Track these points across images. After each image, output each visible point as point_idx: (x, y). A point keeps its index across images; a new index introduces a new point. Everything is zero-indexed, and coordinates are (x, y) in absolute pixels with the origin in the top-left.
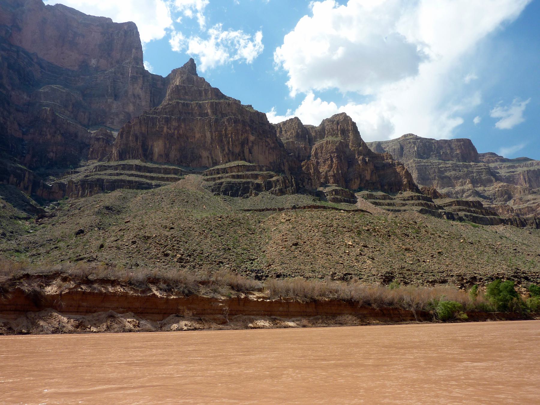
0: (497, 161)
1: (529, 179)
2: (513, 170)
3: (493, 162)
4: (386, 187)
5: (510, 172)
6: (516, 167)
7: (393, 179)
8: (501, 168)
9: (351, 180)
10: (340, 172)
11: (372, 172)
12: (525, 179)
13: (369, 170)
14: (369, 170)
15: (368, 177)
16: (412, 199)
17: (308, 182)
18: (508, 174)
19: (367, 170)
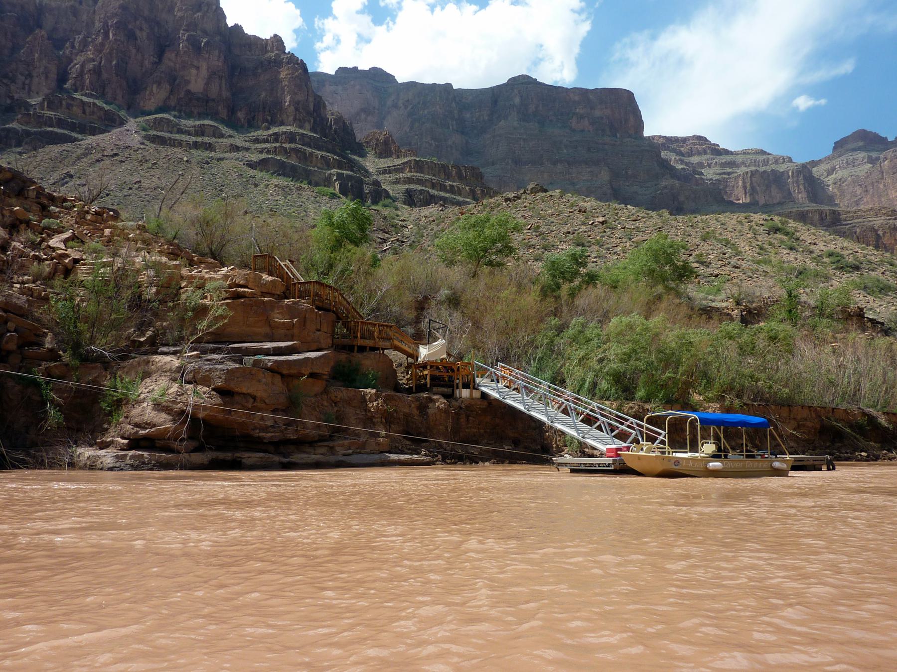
0: (705, 153)
1: (753, 188)
2: (730, 170)
3: (699, 154)
4: (240, 115)
5: (724, 173)
6: (738, 166)
7: (263, 95)
8: (709, 166)
9: (145, 89)
10: (114, 63)
11: (213, 74)
12: (745, 187)
13: (204, 66)
14: (204, 66)
15: (197, 82)
16: (276, 140)
17: (24, 84)
18: (718, 177)
19: (198, 68)
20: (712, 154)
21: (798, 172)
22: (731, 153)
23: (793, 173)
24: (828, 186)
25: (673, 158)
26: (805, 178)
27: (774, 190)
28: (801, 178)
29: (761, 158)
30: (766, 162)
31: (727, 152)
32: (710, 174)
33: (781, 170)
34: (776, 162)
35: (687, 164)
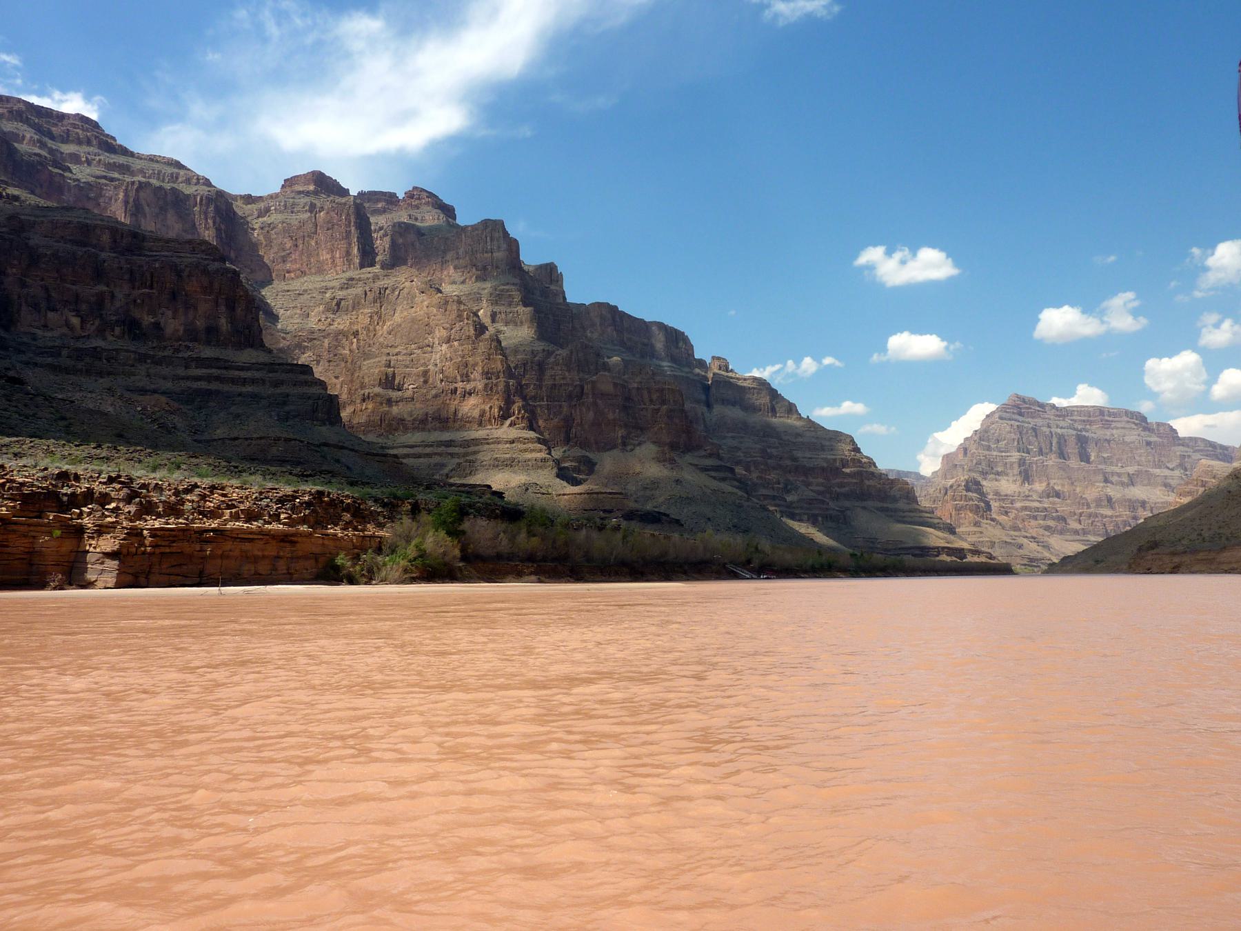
0: (89, 143)
3: (79, 142)
5: (105, 177)
6: (133, 174)
8: (89, 163)
12: (126, 202)
20: (100, 147)
21: (209, 200)
22: (132, 154)
23: (201, 200)
24: (254, 229)
25: (28, 136)
26: (217, 209)
27: (171, 217)
28: (212, 208)
29: (169, 170)
30: (174, 178)
31: (125, 152)
32: (81, 173)
33: (187, 192)
34: (188, 181)
35: (51, 151)
